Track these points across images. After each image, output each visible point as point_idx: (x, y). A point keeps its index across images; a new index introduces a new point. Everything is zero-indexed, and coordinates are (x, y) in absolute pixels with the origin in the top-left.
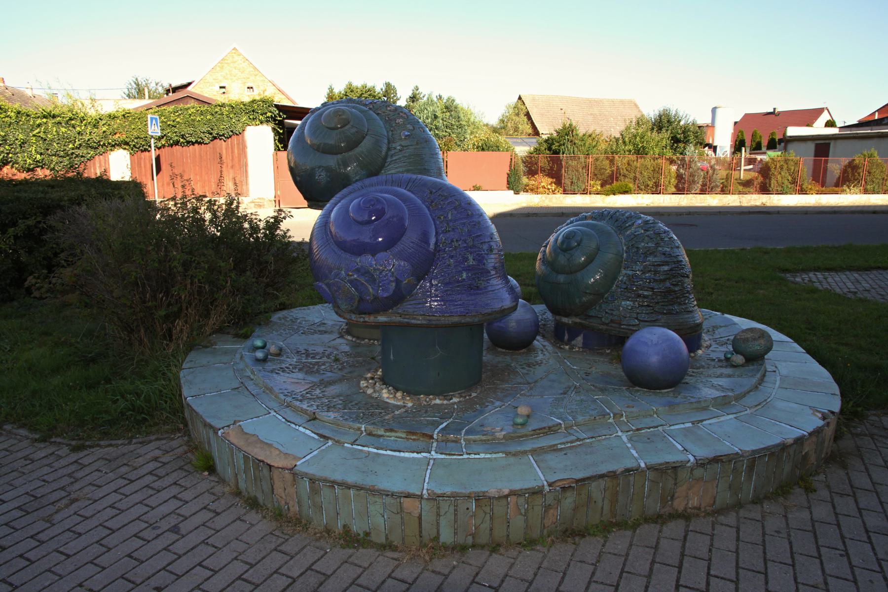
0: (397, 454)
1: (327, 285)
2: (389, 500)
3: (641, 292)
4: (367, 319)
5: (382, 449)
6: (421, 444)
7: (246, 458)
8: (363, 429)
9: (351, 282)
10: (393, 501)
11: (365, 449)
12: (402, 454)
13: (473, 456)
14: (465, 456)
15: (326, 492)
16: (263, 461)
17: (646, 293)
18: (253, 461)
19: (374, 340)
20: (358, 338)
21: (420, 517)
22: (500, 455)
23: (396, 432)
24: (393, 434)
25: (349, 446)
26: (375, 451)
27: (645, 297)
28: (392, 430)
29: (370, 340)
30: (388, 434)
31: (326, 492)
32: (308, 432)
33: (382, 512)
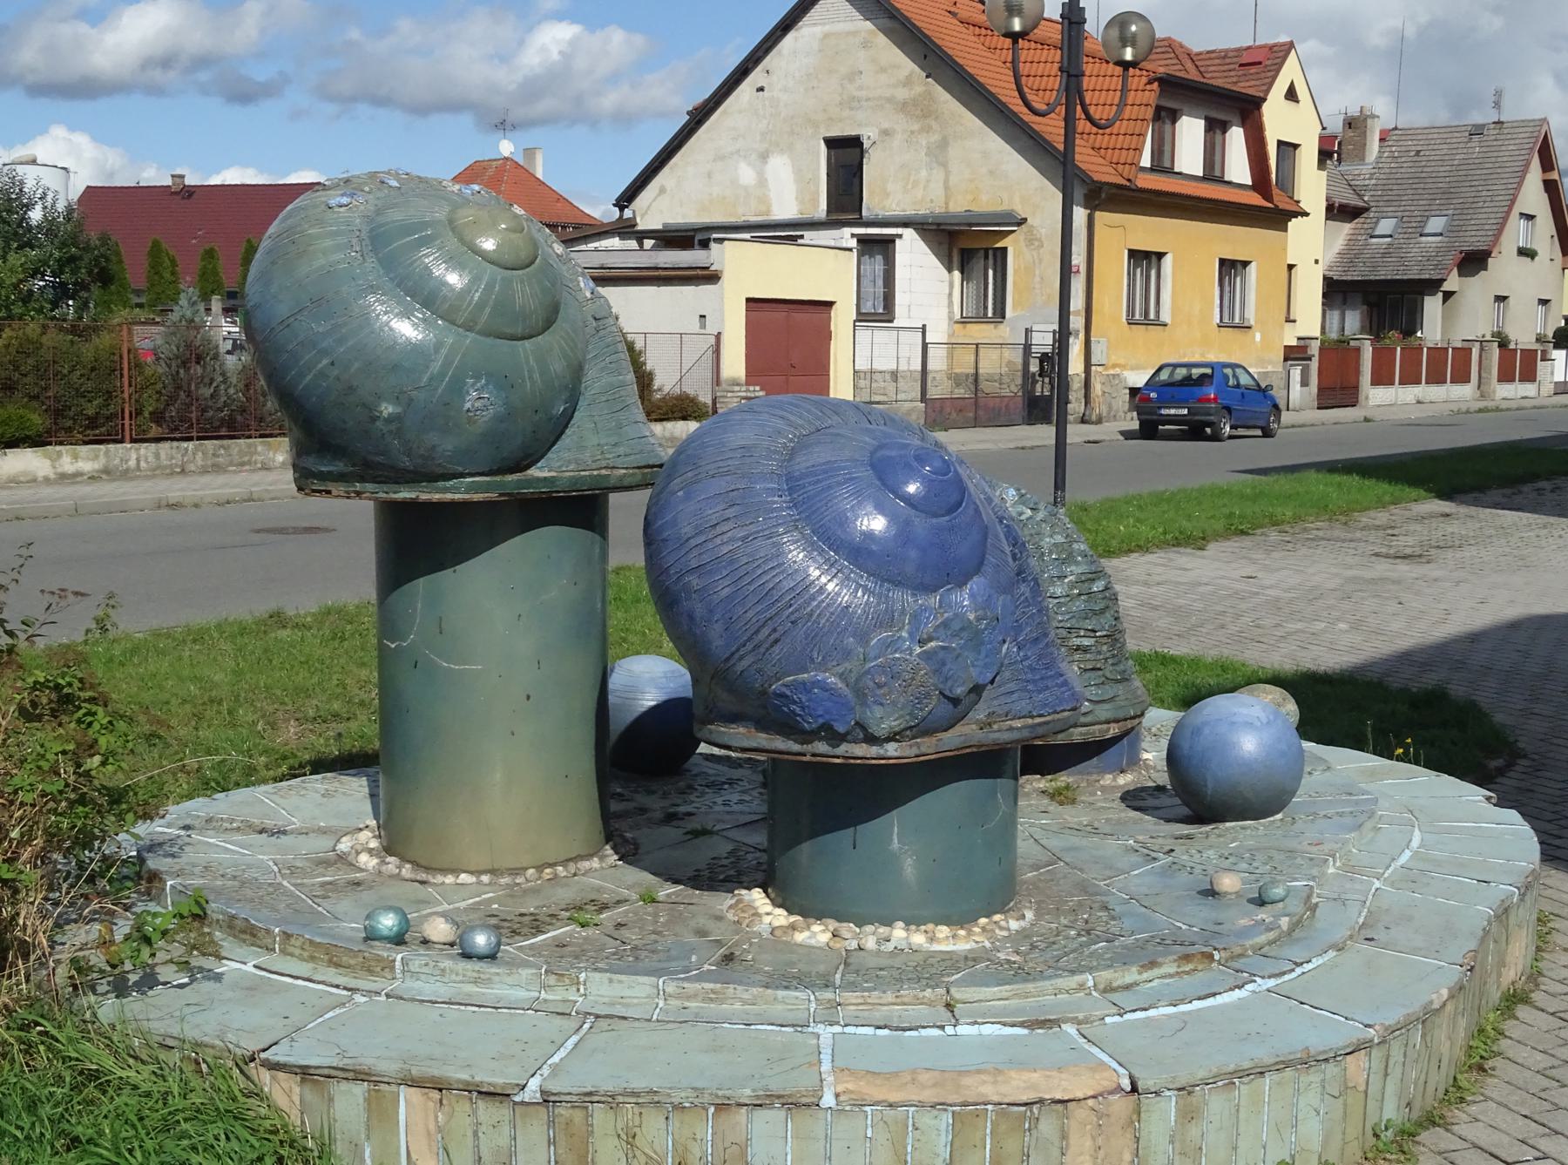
0: (1210, 1002)
1: (841, 676)
2: (1331, 1069)
3: (1077, 641)
4: (924, 750)
5: (1182, 1001)
6: (1203, 977)
7: (966, 1115)
8: (1091, 983)
9: (927, 656)
10: (1336, 1070)
11: (1152, 1013)
12: (1219, 1000)
13: (1307, 967)
14: (1299, 971)
15: (1216, 1105)
16: (1041, 1101)
17: (1086, 642)
18: (1002, 1114)
19: (551, 865)
20: (492, 872)
21: (1366, 1092)
22: (1332, 954)
23: (1159, 965)
24: (1156, 972)
25: (1117, 1019)
26: (1171, 1010)
27: (1085, 650)
28: (1153, 964)
29: (540, 868)
30: (1145, 976)
31: (1216, 1105)
32: (988, 1029)
33: (1316, 1102)
